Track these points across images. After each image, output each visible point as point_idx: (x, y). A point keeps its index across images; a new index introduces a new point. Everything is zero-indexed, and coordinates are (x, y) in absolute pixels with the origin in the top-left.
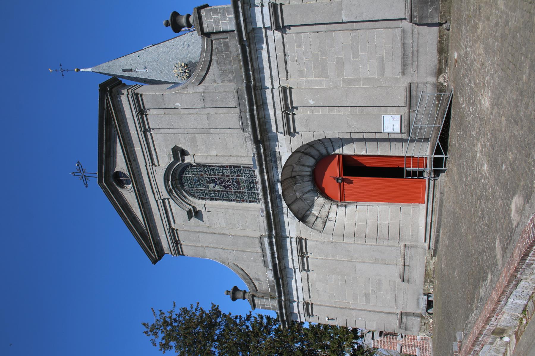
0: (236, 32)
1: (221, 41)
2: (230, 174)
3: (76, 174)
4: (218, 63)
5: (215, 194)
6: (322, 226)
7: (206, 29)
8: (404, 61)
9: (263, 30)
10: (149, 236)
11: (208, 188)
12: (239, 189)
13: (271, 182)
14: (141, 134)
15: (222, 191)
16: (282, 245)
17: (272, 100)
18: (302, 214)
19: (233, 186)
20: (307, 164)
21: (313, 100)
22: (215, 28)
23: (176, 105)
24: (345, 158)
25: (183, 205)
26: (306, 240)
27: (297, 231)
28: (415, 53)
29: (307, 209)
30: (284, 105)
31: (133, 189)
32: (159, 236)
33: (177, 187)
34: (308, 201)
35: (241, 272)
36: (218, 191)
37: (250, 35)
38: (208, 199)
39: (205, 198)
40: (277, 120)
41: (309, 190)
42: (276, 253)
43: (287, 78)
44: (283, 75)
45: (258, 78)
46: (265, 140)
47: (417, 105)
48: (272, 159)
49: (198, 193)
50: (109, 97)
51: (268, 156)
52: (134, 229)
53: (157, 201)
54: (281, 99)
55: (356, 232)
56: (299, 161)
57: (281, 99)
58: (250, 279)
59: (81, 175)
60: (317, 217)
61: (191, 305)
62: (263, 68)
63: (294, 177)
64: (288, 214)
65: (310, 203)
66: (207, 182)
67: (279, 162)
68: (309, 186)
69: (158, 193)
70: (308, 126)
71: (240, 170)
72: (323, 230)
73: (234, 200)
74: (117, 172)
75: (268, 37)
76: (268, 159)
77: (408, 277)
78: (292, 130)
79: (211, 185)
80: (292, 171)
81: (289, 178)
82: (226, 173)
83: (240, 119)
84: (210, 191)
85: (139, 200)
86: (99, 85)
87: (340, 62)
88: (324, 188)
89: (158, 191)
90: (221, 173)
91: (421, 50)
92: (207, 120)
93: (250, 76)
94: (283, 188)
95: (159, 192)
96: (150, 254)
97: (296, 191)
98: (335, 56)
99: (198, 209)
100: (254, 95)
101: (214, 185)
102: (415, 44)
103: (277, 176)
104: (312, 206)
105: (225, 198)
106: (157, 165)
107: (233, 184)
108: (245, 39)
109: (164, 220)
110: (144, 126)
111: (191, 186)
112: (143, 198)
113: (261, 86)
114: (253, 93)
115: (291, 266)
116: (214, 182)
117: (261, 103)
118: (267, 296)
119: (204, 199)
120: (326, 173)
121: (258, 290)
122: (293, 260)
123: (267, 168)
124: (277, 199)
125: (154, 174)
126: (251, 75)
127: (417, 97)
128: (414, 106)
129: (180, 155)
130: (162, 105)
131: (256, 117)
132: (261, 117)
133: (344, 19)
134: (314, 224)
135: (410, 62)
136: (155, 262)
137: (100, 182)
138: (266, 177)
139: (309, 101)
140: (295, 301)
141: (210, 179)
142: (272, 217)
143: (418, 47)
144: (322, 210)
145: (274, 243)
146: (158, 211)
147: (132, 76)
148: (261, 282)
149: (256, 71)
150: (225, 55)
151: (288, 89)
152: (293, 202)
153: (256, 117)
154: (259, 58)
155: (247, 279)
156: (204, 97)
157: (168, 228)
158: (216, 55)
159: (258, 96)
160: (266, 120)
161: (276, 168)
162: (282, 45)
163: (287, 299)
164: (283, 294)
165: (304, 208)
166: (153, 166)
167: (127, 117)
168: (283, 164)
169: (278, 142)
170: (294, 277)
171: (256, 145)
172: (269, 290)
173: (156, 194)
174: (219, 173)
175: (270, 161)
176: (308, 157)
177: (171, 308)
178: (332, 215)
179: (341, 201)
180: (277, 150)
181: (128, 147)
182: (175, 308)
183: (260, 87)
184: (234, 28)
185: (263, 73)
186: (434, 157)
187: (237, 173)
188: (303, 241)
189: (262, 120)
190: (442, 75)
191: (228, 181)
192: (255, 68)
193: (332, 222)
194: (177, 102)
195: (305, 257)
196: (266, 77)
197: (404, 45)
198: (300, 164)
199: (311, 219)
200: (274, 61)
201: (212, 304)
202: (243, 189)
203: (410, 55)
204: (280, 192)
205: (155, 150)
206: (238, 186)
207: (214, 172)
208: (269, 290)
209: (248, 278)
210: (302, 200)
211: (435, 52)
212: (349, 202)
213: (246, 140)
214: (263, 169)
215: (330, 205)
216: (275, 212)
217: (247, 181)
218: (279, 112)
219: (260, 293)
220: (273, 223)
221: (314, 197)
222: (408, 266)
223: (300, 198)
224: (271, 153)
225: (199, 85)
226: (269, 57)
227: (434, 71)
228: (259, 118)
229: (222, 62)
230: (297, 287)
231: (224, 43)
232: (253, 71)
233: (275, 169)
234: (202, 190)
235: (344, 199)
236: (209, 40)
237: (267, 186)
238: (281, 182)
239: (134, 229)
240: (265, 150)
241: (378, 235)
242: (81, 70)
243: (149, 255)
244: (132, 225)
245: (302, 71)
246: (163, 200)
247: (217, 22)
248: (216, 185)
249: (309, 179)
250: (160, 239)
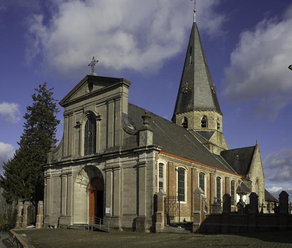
4: (131, 137)
44: (125, 166)
78: (107, 170)
79: (89, 133)
133: (140, 192)
138: (91, 159)
178: (83, 186)
184: (140, 146)
197: (132, 215)
218: (112, 165)
246: (83, 109)
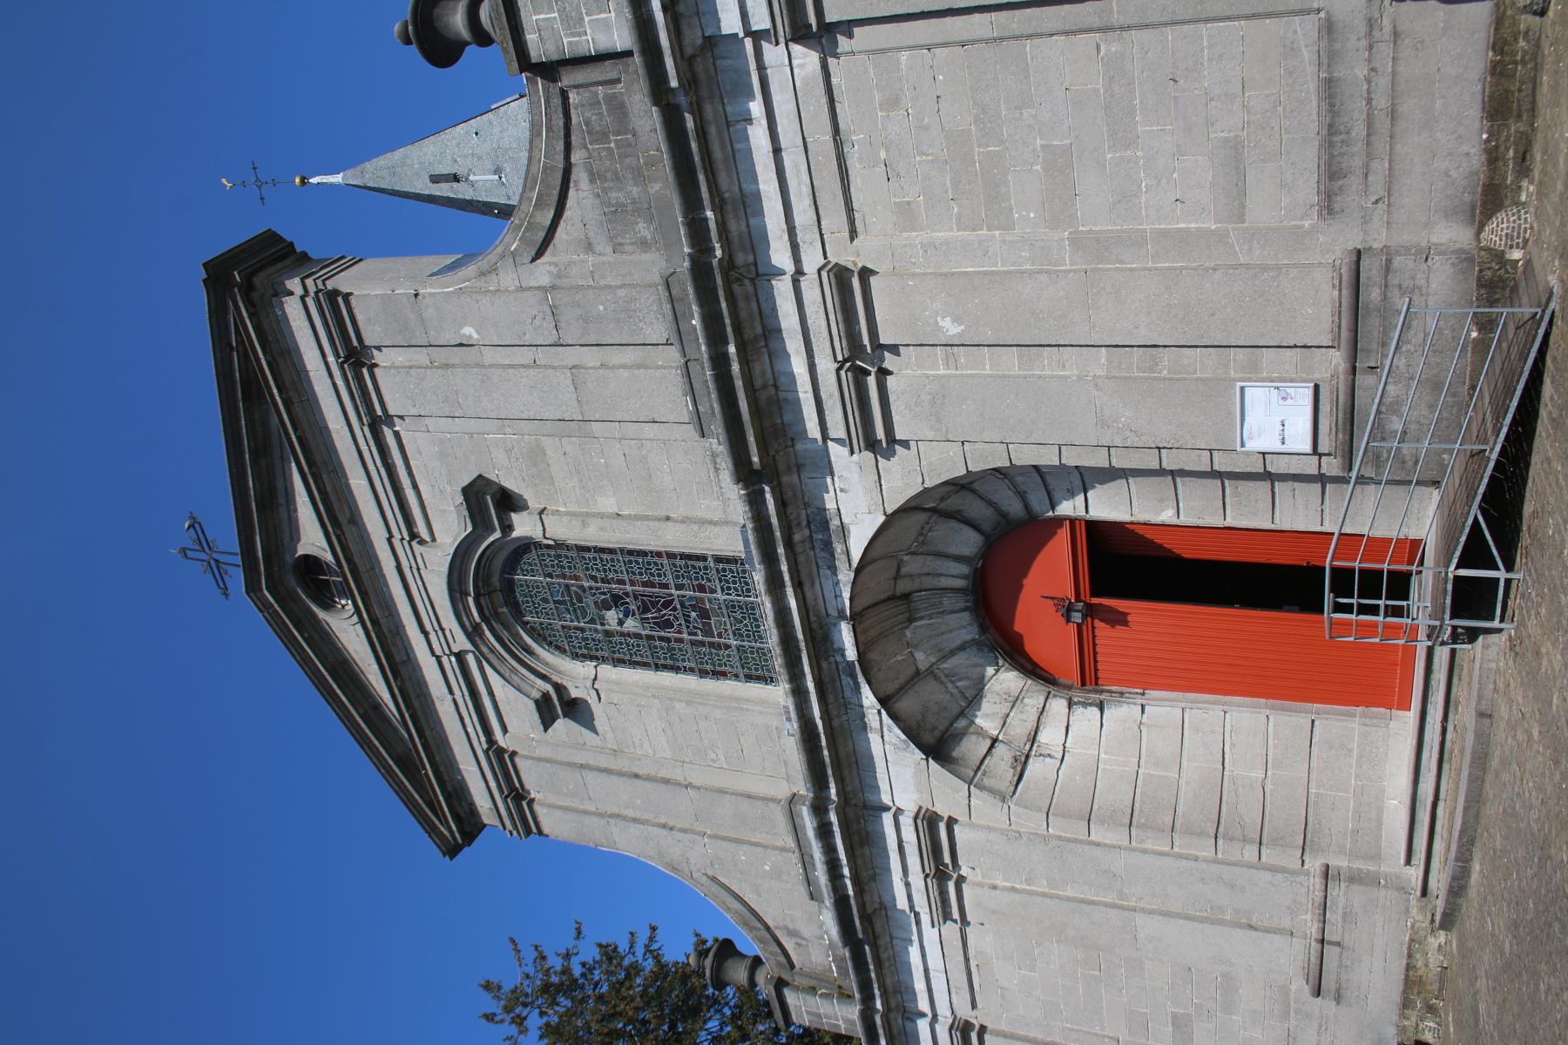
0: (637, 59)
1: (596, 94)
2: (670, 579)
3: (190, 554)
5: (628, 645)
6: (1009, 775)
7: (538, 48)
8: (1332, 156)
9: (748, 43)
10: (425, 768)
11: (603, 624)
12: (708, 632)
13: (813, 619)
14: (363, 434)
15: (650, 638)
16: (867, 833)
17: (796, 319)
18: (935, 728)
20: (953, 550)
21: (957, 320)
22: (570, 44)
23: (465, 335)
24: (1098, 535)
25: (523, 678)
26: (951, 822)
27: (919, 791)
28: (1383, 124)
29: (956, 710)
30: (844, 341)
31: (355, 619)
32: (459, 770)
33: (497, 615)
34: (960, 680)
35: (736, 905)
36: (637, 636)
37: (699, 67)
38: (604, 660)
39: (597, 658)
40: (823, 395)
41: (966, 642)
42: (844, 861)
43: (853, 234)
44: (835, 221)
45: (740, 235)
46: (781, 466)
47: (1384, 344)
48: (814, 535)
49: (571, 637)
50: (241, 305)
51: (799, 524)
52: (376, 742)
53: (438, 659)
54: (832, 317)
55: (1137, 805)
56: (921, 538)
57: (832, 317)
58: (768, 928)
59: (207, 558)
60: (995, 741)
61: (632, 934)
62: (757, 196)
63: (906, 597)
64: (885, 729)
65: (968, 687)
66: (596, 603)
67: (839, 548)
68: (962, 627)
69: (440, 633)
70: (939, 421)
71: (706, 568)
72: (1014, 793)
73: (692, 670)
74: (306, 557)
75: (769, 71)
76: (797, 537)
77: (1338, 982)
78: (880, 433)
79: (612, 616)
80: (897, 576)
81: (884, 601)
82: (659, 575)
83: (688, 388)
84: (608, 634)
85: (381, 655)
86: (205, 265)
87: (1059, 165)
88: (1021, 636)
89: (437, 628)
90: (641, 574)
91: (1408, 107)
92: (572, 389)
93: (708, 230)
94: (862, 638)
95: (443, 630)
96: (435, 826)
97: (916, 647)
98: (1038, 141)
99: (574, 693)
100: (726, 299)
101: (621, 616)
102: (1382, 82)
103: (836, 596)
104: (974, 699)
105: (663, 662)
106: (428, 539)
107: (687, 617)
108: (674, 83)
109: (467, 720)
110: (367, 405)
111: (547, 614)
112: (395, 645)
113: (756, 264)
114: (721, 293)
115: (902, 903)
116: (622, 604)
117: (759, 330)
118: (826, 988)
119: (591, 658)
120: (1025, 582)
121: (798, 966)
122: (908, 885)
123: (798, 571)
124: (843, 677)
125: (418, 569)
126: (712, 225)
127: (1386, 312)
128: (1374, 346)
129: (493, 512)
130: (417, 333)
131: (739, 384)
132: (758, 382)
134: (983, 767)
135: (1357, 162)
136: (452, 851)
137: (252, 587)
138: (793, 603)
139: (941, 323)
140: (923, 1015)
141: (604, 594)
142: (824, 743)
143: (1394, 95)
144: (1012, 714)
145: (836, 829)
146: (446, 691)
147: (460, 196)
148: (804, 943)
149: (729, 207)
150: (618, 148)
151: (856, 275)
152: (902, 689)
153: (739, 384)
154: (740, 157)
155: (756, 929)
156: (555, 306)
157: (485, 746)
158: (586, 147)
159: (742, 304)
160: (782, 395)
161: (829, 568)
162: (824, 100)
163: (893, 1006)
164: (877, 992)
165: (945, 708)
166: (414, 543)
167: (311, 374)
168: (856, 555)
169: (832, 474)
170: (915, 938)
171: (746, 488)
172: (834, 968)
173: (433, 637)
174: (634, 573)
175: (808, 545)
176: (953, 524)
177: (568, 942)
178: (1050, 736)
179: (1083, 684)
180: (830, 505)
181: (324, 476)
182: (581, 943)
183: (753, 269)
185: (760, 212)
186: (1456, 578)
187: (697, 578)
188: (942, 827)
189: (763, 396)
190: (1501, 215)
191: (667, 604)
192: (727, 195)
193: (1048, 760)
194: (466, 325)
195: (950, 877)
196: (770, 227)
197: (1329, 88)
198: (922, 547)
199: (971, 748)
200: (796, 166)
201: (697, 935)
202: (720, 635)
203: (1359, 130)
204: (851, 653)
205: (415, 487)
206: (704, 624)
207: (616, 571)
208: (834, 968)
209: (759, 925)
210: (936, 678)
211: (1473, 115)
212: (1114, 688)
213: (715, 463)
214: (781, 573)
215: (1042, 699)
216: (836, 723)
217: (734, 607)
218: (826, 366)
219: (800, 975)
220: (827, 760)
221: (983, 666)
222: (1338, 944)
223: (930, 672)
224: (808, 516)
225: (533, 260)
226: (777, 151)
227: (1467, 198)
228: (753, 386)
229: (609, 175)
230: (926, 971)
231: (610, 99)
232: (720, 206)
233: (828, 572)
234: (582, 630)
235: (1097, 679)
236: (555, 89)
237: (800, 636)
238: (853, 618)
239: (376, 742)
240: (782, 505)
241: (1222, 821)
242: (314, 180)
243: (431, 830)
244: (367, 731)
245: (909, 203)
246: (460, 657)
247: (573, 22)
249: (961, 605)
250: (463, 778)
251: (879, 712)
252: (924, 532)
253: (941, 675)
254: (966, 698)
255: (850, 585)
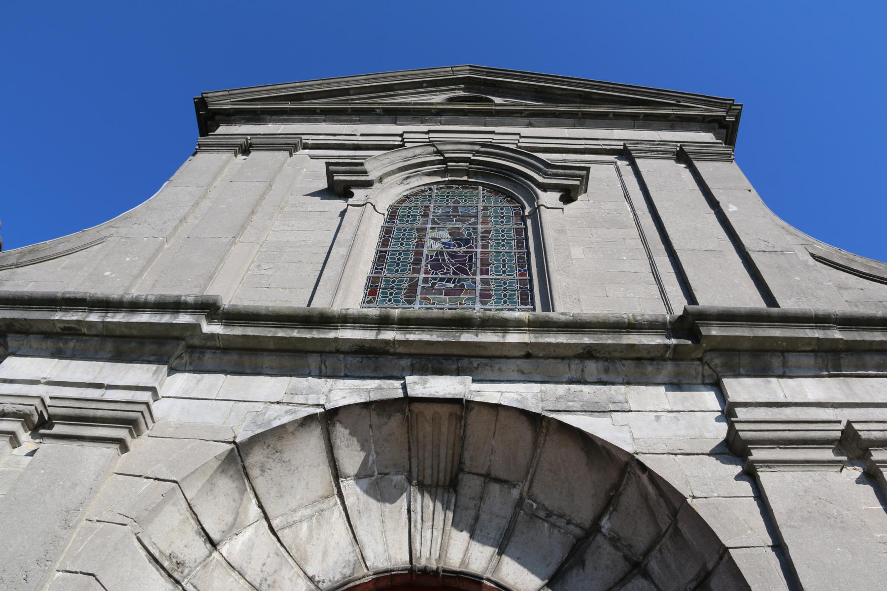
6: (160, 544)
11: (432, 228)
19: (442, 280)
34: (310, 529)
53: (401, 135)
56: (542, 514)
69: (428, 140)
80: (489, 478)
101: (443, 240)
141: (469, 234)
144: (242, 581)
165: (281, 496)
225: (813, 256)
228: (789, 351)
248: (444, 243)
251: (318, 405)
252: (553, 519)
253: (324, 506)
254: (283, 528)
255: (521, 407)
